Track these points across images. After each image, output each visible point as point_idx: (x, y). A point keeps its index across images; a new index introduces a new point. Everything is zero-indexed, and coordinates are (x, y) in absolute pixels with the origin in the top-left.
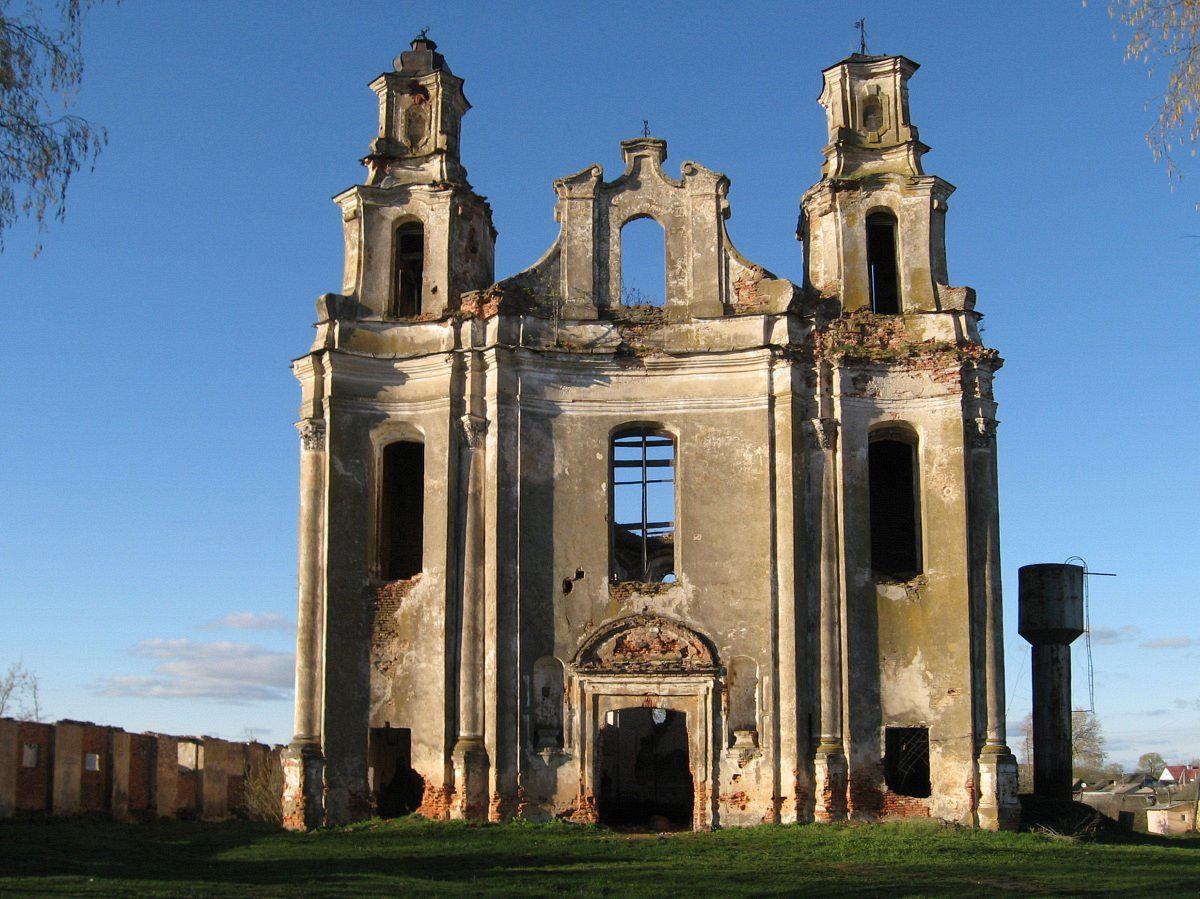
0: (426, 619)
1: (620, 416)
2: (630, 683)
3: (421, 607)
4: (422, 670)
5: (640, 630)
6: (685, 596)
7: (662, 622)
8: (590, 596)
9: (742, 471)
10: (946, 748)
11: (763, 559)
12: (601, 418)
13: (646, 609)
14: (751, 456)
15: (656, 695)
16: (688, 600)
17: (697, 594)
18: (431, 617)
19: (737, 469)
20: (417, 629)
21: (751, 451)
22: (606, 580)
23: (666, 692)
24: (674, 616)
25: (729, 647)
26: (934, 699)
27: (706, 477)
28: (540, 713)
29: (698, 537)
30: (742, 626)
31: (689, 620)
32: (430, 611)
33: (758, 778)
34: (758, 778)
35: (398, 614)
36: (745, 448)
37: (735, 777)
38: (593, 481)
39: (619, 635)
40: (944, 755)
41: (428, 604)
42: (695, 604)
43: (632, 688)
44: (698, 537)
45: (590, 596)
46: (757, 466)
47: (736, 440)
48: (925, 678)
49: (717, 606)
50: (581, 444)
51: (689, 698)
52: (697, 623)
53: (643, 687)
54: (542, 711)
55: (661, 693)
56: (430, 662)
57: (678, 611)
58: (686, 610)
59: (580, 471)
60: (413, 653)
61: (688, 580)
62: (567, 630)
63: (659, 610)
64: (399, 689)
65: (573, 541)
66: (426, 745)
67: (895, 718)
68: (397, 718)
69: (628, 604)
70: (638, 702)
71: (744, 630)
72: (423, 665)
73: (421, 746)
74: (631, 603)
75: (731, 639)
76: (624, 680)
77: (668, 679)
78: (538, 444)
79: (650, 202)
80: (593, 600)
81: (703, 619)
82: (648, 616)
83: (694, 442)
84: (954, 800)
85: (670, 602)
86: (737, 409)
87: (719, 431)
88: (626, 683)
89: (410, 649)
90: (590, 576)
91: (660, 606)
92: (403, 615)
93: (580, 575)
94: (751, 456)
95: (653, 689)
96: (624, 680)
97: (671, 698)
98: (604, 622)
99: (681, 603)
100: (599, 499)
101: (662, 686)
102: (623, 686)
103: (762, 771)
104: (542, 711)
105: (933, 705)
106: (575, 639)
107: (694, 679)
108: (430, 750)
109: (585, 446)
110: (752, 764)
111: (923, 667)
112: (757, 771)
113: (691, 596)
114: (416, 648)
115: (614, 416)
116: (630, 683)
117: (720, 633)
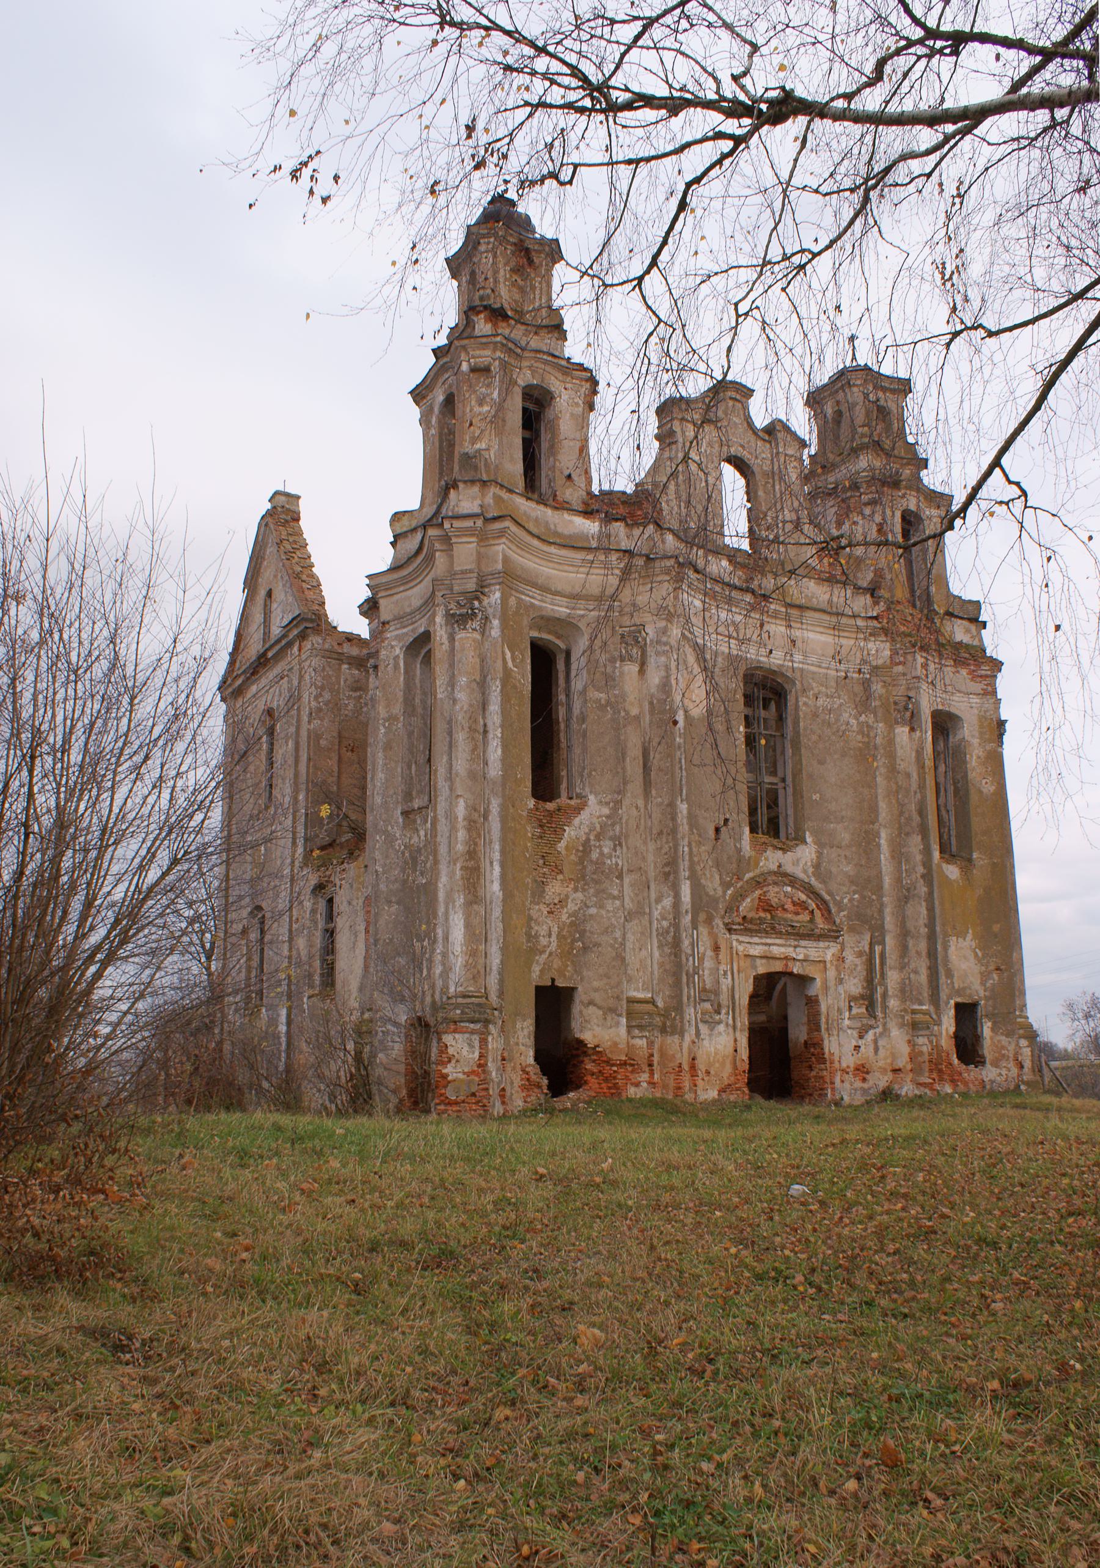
0: (595, 855)
3: (588, 840)
4: (591, 915)
7: (792, 880)
10: (994, 1023)
13: (780, 866)
17: (820, 855)
18: (602, 854)
20: (584, 867)
22: (747, 830)
23: (801, 957)
24: (802, 876)
26: (984, 977)
29: (816, 797)
30: (855, 893)
31: (813, 881)
32: (600, 847)
33: (876, 1050)
34: (876, 1050)
35: (561, 846)
37: (857, 1048)
40: (992, 1029)
41: (598, 838)
42: (817, 866)
43: (776, 951)
44: (816, 797)
46: (861, 732)
48: (976, 955)
49: (834, 870)
53: (782, 950)
56: (602, 907)
57: (805, 871)
58: (811, 870)
60: (579, 895)
63: (789, 868)
64: (564, 937)
66: (599, 1008)
67: (959, 992)
68: (561, 972)
70: (778, 967)
72: (593, 911)
73: (592, 1009)
76: (769, 941)
77: (803, 943)
79: (742, 446)
82: (783, 876)
84: (1004, 1072)
89: (576, 890)
92: (567, 848)
93: (726, 821)
95: (790, 952)
96: (769, 941)
103: (881, 1043)
105: (983, 983)
106: (724, 893)
107: (821, 944)
108: (605, 1014)
110: (870, 1036)
111: (974, 944)
112: (875, 1041)
113: (814, 856)
114: (584, 890)
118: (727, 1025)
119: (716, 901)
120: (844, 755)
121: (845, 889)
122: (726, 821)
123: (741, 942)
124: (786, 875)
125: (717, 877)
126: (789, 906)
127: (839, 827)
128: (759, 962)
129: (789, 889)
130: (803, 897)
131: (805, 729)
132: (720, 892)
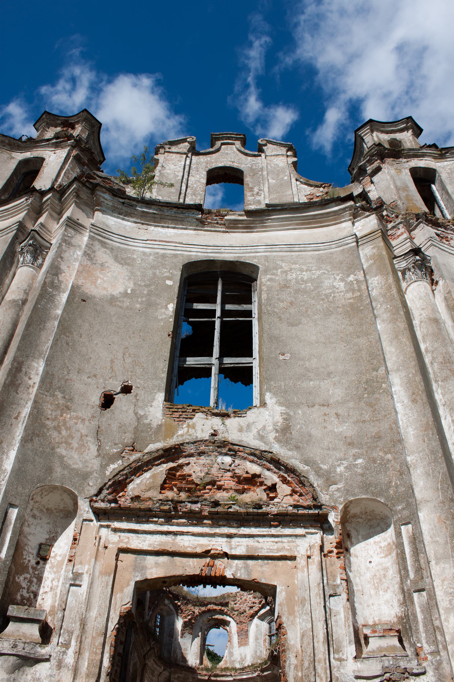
1: (196, 256)
2: (182, 533)
5: (203, 460)
6: (270, 419)
8: (136, 414)
9: (334, 297)
11: (375, 373)
12: (175, 256)
13: (214, 435)
14: (342, 284)
15: (226, 555)
16: (275, 424)
17: (287, 419)
19: (327, 296)
21: (342, 280)
22: (161, 396)
25: (340, 485)
27: (291, 303)
28: (24, 584)
30: (356, 457)
36: (335, 279)
38: (158, 301)
39: (171, 465)
45: (136, 414)
47: (324, 273)
49: (316, 432)
50: (150, 273)
51: (280, 563)
52: (290, 453)
53: (204, 541)
54: (31, 582)
55: (234, 552)
57: (261, 438)
58: (272, 436)
59: (145, 292)
61: (274, 400)
62: (96, 453)
65: (124, 354)
69: (188, 426)
71: (360, 461)
74: (193, 427)
75: (341, 475)
78: (102, 265)
80: (139, 419)
81: (297, 448)
83: (277, 275)
85: (249, 426)
86: (321, 252)
87: (305, 268)
88: (175, 534)
90: (141, 392)
91: (235, 431)
94: (342, 284)
97: (250, 562)
98: (152, 447)
99: (264, 427)
100: (164, 316)
101: (235, 541)
102: (169, 538)
104: (31, 582)
106: (103, 467)
109: (154, 274)
113: (279, 419)
115: (190, 256)
116: (182, 533)
117: (325, 467)
118: (60, 665)
119: (85, 476)
120: (328, 313)
121: (339, 455)
122: (127, 390)
123: (115, 530)
124: (224, 444)
125: (93, 449)
126: (228, 482)
127: (325, 384)
128: (151, 559)
129: (228, 460)
130: (255, 469)
131: (268, 299)
132: (95, 464)
